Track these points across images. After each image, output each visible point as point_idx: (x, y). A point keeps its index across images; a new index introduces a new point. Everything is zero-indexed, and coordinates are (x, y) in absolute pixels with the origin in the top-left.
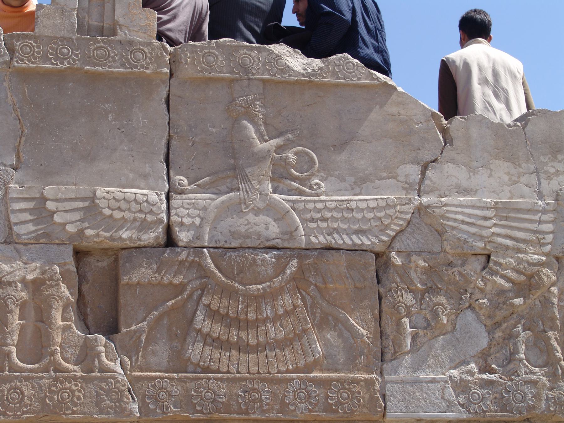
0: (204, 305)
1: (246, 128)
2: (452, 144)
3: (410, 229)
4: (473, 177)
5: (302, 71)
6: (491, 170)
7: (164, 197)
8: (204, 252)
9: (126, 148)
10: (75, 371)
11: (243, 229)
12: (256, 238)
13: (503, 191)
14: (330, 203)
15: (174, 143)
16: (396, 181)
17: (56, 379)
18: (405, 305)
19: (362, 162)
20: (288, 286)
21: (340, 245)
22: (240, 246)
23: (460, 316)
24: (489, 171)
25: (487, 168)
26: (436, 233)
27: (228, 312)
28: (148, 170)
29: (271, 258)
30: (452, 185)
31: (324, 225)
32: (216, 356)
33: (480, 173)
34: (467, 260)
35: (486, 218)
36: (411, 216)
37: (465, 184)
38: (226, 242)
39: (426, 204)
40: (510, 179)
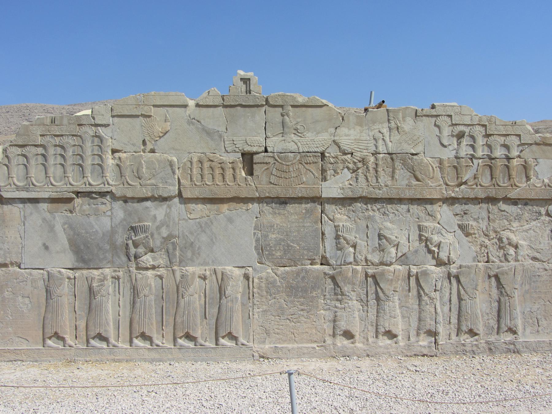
11: (285, 148)
15: (267, 124)
31: (307, 146)
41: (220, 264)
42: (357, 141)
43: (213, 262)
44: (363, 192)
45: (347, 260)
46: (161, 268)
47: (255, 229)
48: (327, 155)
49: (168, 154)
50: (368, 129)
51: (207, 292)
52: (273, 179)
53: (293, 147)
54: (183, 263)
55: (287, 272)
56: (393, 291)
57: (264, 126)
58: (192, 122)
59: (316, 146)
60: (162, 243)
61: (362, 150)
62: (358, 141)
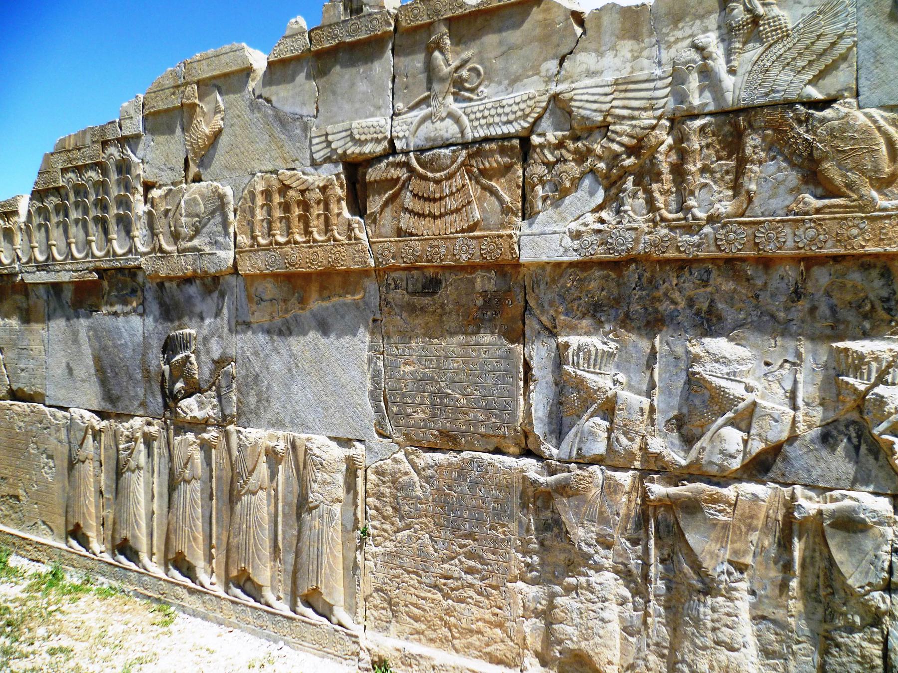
11: (432, 134)
17: (334, 246)
31: (483, 121)
35: (606, 95)
37: (593, 68)
41: (306, 428)
43: (292, 421)
44: (636, 240)
45: (584, 449)
46: (212, 425)
47: (370, 351)
48: (536, 140)
49: (220, 181)
51: (280, 488)
52: (406, 221)
53: (448, 129)
54: (243, 420)
55: (438, 465)
56: (730, 562)
57: (390, 86)
58: (257, 104)
60: (212, 373)
62: (622, 85)
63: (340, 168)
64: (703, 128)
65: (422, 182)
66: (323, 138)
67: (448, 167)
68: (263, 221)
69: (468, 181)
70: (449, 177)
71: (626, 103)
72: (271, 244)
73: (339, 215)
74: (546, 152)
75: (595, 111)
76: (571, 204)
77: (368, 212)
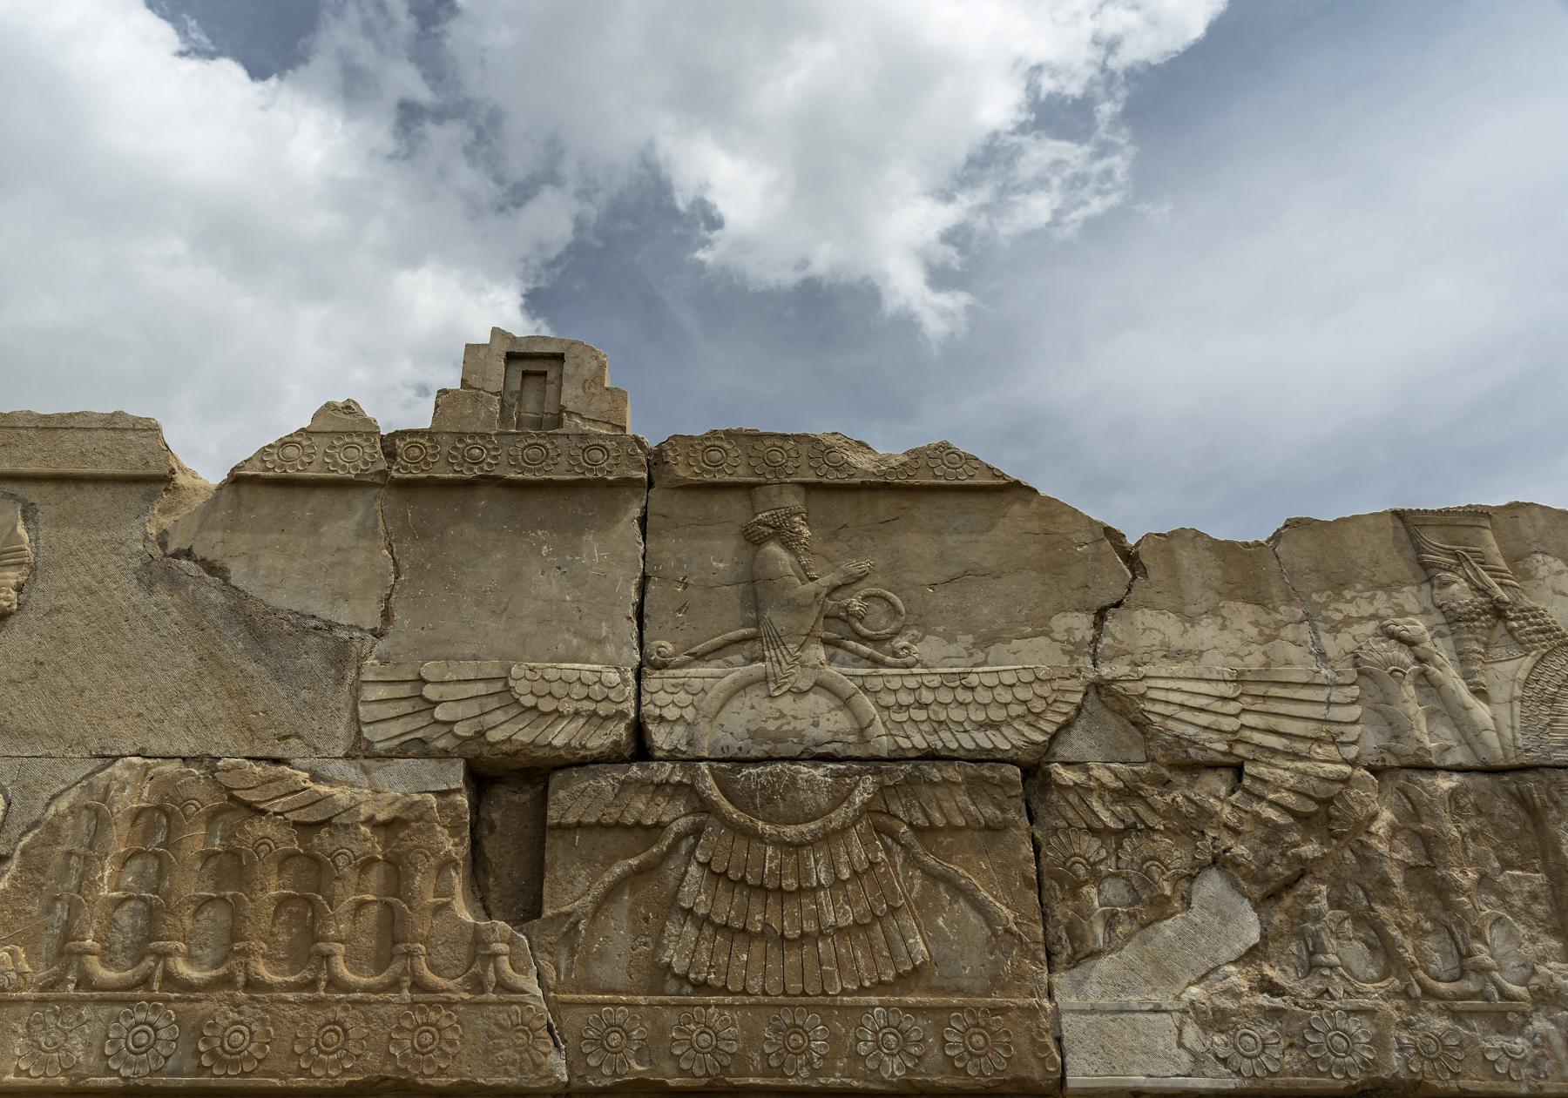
0: (699, 863)
1: (776, 559)
2: (1145, 574)
3: (1083, 722)
4: (1191, 630)
5: (872, 470)
6: (1223, 617)
7: (630, 675)
8: (699, 768)
9: (568, 598)
10: (449, 990)
11: (771, 726)
12: (795, 740)
13: (1249, 654)
14: (930, 678)
15: (651, 587)
16: (1049, 640)
18: (1086, 859)
19: (986, 611)
20: (858, 827)
21: (953, 751)
22: (766, 756)
23: (1198, 881)
24: (1220, 620)
25: (1216, 616)
26: (1132, 727)
27: (745, 875)
28: (604, 630)
29: (826, 776)
30: (1153, 645)
31: (920, 715)
32: (721, 962)
33: (1202, 623)
34: (1197, 778)
35: (1224, 699)
36: (1084, 699)
37: (1177, 643)
38: (740, 749)
39: (1110, 677)
40: (1261, 633)
42: (1260, 690)
50: (1308, 617)
57: (635, 598)
58: (168, 570)
59: (980, 716)
61: (1300, 747)
63: (455, 775)
64: (1454, 794)
65: (740, 844)
66: (405, 690)
67: (821, 813)
68: (119, 903)
69: (881, 855)
70: (829, 838)
71: (1273, 722)
72: (145, 982)
73: (438, 909)
74: (1097, 806)
75: (1206, 728)
76: (1180, 935)
77: (548, 912)
